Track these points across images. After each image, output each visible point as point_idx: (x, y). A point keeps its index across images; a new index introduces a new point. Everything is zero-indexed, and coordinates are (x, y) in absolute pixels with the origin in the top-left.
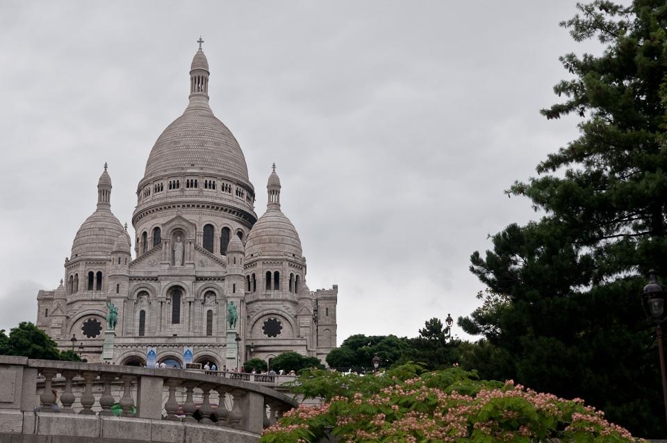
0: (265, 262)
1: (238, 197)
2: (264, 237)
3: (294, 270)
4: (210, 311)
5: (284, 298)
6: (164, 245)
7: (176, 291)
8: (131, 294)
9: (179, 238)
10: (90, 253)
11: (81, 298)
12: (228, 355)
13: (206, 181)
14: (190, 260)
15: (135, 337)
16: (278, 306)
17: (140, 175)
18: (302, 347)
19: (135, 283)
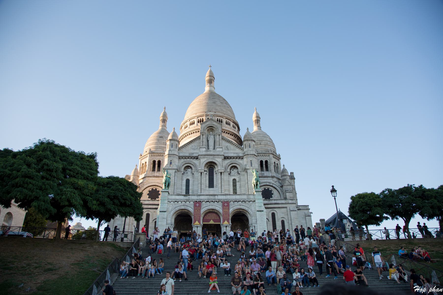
0: (259, 154)
4: (234, 180)
5: (273, 176)
6: (202, 136)
7: (211, 166)
8: (180, 168)
9: (211, 132)
11: (148, 175)
12: (258, 209)
13: (218, 119)
14: (219, 146)
15: (182, 195)
16: (269, 180)
18: (293, 205)
19: (182, 160)
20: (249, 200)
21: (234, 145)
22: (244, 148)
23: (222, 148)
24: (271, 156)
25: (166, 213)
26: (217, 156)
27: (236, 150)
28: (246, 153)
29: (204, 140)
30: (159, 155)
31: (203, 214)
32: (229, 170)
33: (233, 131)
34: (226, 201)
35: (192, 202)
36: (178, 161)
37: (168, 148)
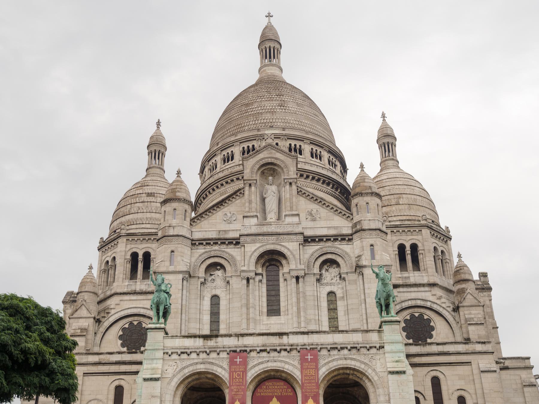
1: (331, 167)
2: (386, 198)
3: (437, 242)
4: (331, 294)
5: (432, 281)
6: (247, 188)
9: (270, 178)
10: (133, 227)
11: (119, 291)
13: (290, 145)
15: (200, 336)
17: (205, 147)
18: (485, 356)
19: (201, 250)
20: (368, 346)
21: (328, 208)
22: (355, 214)
23: (298, 215)
24: (426, 232)
25: (159, 383)
26: (285, 236)
27: (333, 220)
28: (358, 227)
29: (253, 197)
30: (147, 238)
31: (254, 384)
32: (319, 270)
33: (330, 174)
34: (308, 348)
35: (225, 353)
36: (189, 253)
37: (165, 221)
